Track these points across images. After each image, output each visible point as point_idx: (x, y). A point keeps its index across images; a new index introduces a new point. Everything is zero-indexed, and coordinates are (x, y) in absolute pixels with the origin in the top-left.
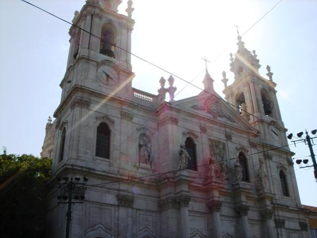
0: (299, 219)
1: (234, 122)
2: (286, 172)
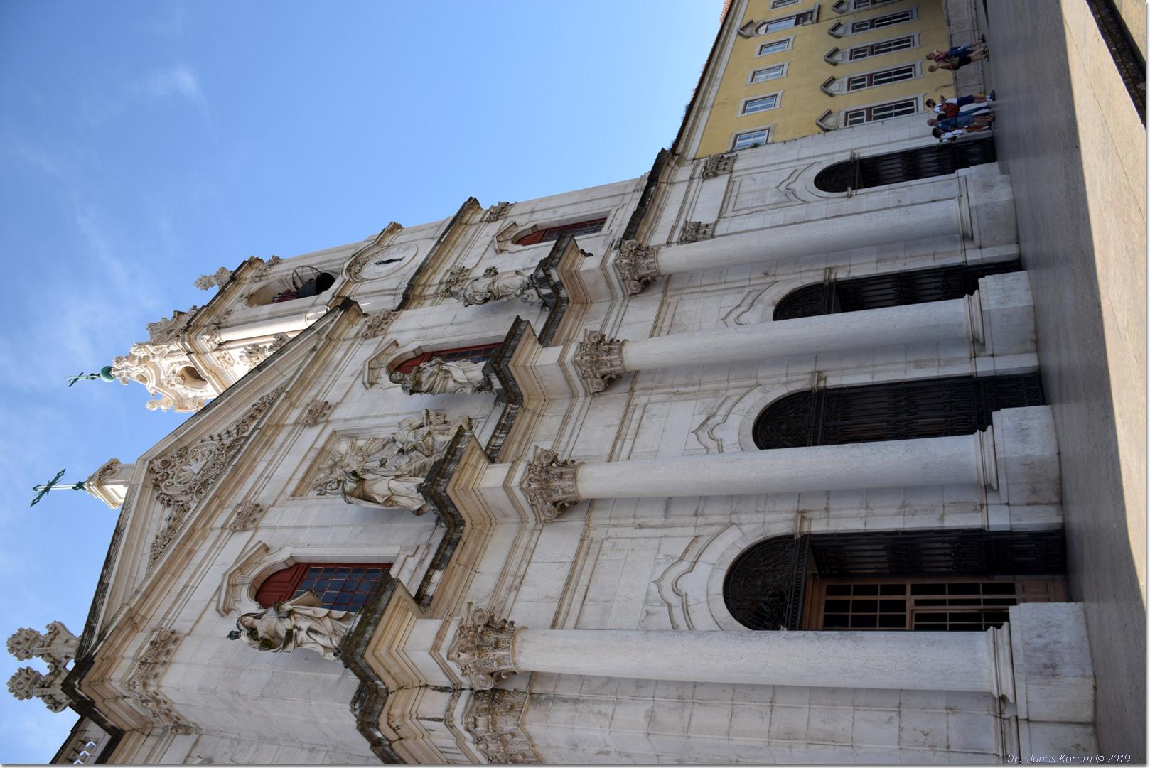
0: (692, 178)
2: (525, 223)
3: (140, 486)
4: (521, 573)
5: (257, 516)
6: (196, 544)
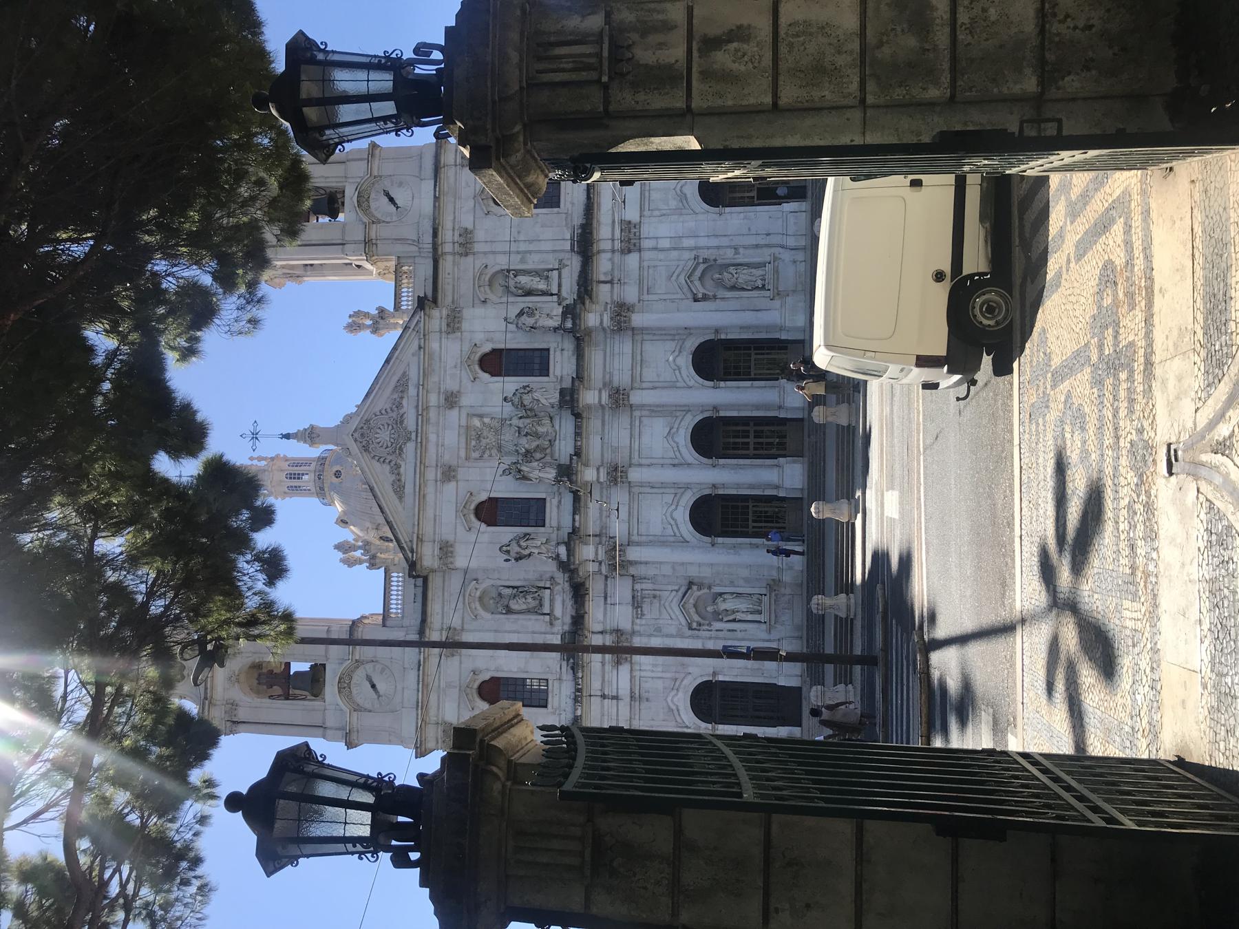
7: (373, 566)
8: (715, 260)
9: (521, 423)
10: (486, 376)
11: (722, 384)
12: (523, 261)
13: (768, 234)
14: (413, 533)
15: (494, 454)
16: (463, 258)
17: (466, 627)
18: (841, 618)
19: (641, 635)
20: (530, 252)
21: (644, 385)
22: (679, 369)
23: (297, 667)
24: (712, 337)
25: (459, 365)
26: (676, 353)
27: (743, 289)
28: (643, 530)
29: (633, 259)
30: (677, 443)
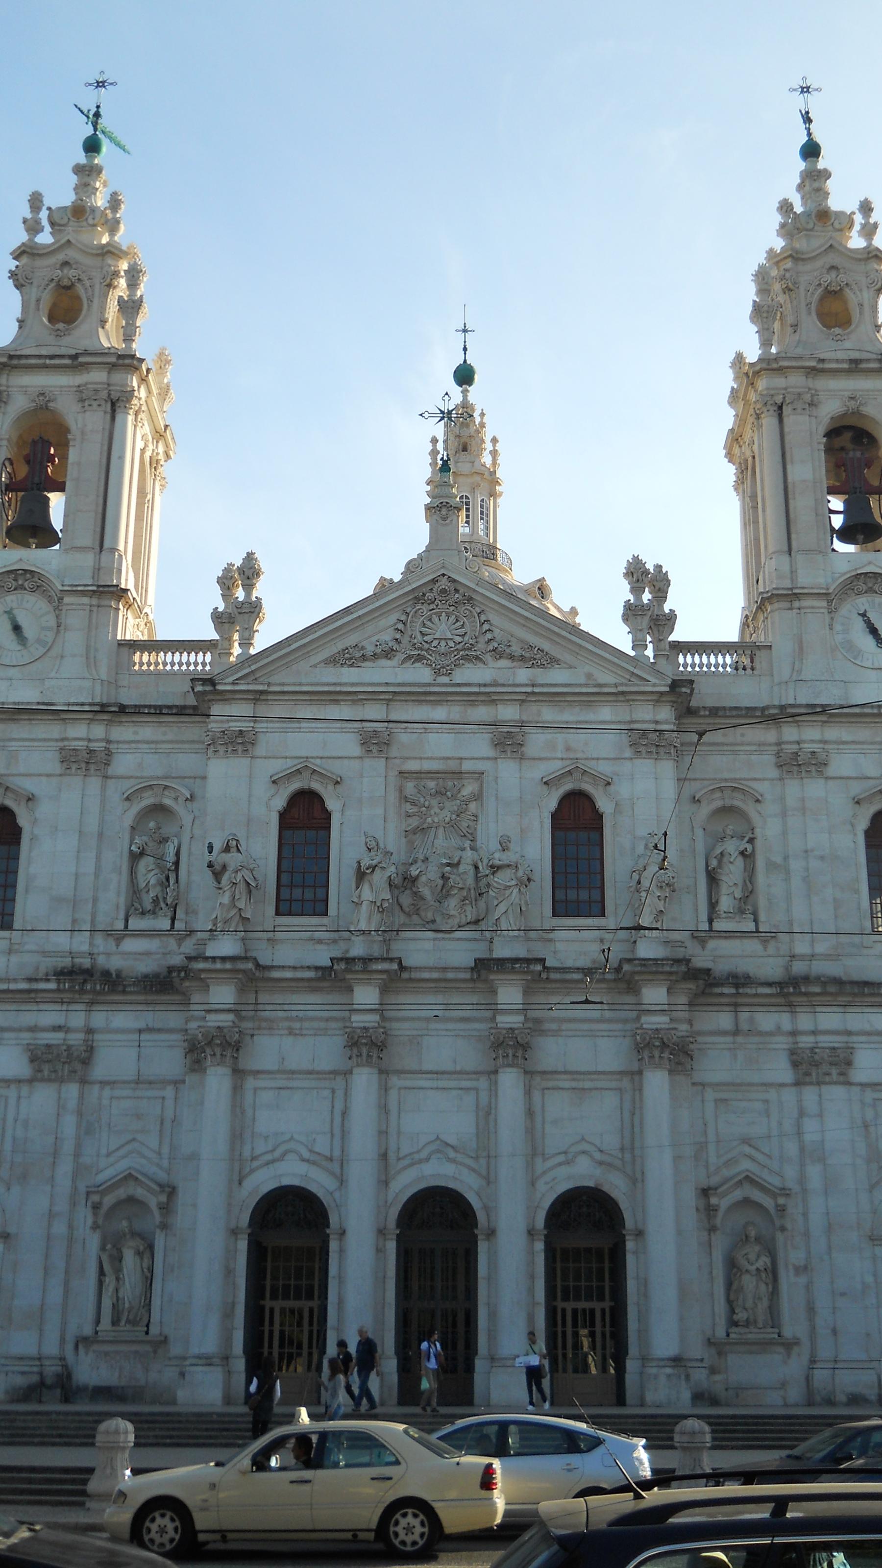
1: (554, 661)
3: (409, 588)
4: (305, 1032)
5: (374, 751)
6: (346, 700)
7: (218, 618)
8: (783, 1229)
9: (466, 867)
10: (553, 804)
11: (540, 1246)
12: (771, 866)
13: (834, 1332)
14: (269, 684)
15: (410, 820)
16: (773, 759)
17: (110, 783)
18: (85, 1482)
19: (81, 1097)
20: (787, 880)
21: (537, 1096)
22: (567, 1163)
23: (56, 502)
24: (629, 1223)
25: (572, 756)
26: (598, 1156)
27: (729, 1285)
28: (266, 1097)
29: (781, 1070)
30: (427, 1159)
